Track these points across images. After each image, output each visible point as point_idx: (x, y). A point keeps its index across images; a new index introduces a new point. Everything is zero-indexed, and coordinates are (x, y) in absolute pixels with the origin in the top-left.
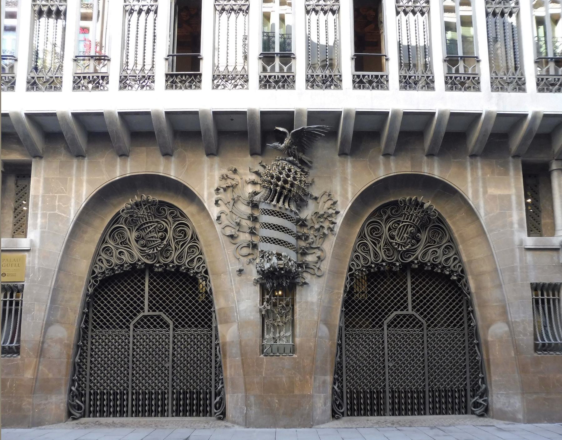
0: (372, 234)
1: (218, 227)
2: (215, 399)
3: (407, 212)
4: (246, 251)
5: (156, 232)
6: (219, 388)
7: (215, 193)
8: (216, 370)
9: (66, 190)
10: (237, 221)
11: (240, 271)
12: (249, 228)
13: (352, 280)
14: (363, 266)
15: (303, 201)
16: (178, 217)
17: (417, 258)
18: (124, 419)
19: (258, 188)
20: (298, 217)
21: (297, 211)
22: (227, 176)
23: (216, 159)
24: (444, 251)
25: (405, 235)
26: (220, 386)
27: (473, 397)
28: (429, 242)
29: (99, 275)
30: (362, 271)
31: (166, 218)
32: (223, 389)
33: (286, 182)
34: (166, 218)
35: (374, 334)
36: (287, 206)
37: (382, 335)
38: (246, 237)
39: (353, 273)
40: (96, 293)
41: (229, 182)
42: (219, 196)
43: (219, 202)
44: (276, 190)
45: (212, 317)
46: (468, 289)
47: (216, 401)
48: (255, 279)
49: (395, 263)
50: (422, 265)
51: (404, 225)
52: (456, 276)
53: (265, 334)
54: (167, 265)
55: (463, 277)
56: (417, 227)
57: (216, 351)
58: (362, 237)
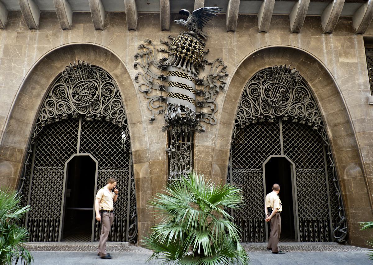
0: (252, 94)
1: (136, 85)
2: (130, 226)
3: (278, 76)
4: (157, 104)
5: (88, 90)
6: (133, 217)
7: (134, 59)
8: (131, 202)
9: (21, 55)
10: (150, 80)
11: (152, 120)
12: (160, 87)
13: (237, 129)
14: (246, 119)
15: (201, 66)
16: (106, 78)
17: (287, 113)
18: (54, 244)
19: (166, 56)
20: (197, 78)
21: (197, 74)
22: (143, 46)
23: (136, 33)
24: (307, 108)
25: (278, 94)
26: (134, 215)
27: (335, 227)
28: (295, 100)
29: (43, 123)
30: (246, 122)
31: (97, 79)
32: (136, 218)
33: (188, 50)
34: (97, 79)
35: (255, 173)
36: (189, 69)
37: (261, 174)
38: (157, 94)
39: (239, 124)
40: (40, 137)
41: (145, 50)
42: (137, 61)
43: (138, 66)
44: (180, 57)
45: (129, 158)
46: (327, 138)
47: (130, 228)
48: (163, 127)
49: (271, 116)
50: (290, 118)
51: (277, 87)
52: (317, 127)
53: (171, 172)
54: (95, 116)
55: (322, 128)
56: (286, 88)
57: (132, 186)
58: (245, 96)
